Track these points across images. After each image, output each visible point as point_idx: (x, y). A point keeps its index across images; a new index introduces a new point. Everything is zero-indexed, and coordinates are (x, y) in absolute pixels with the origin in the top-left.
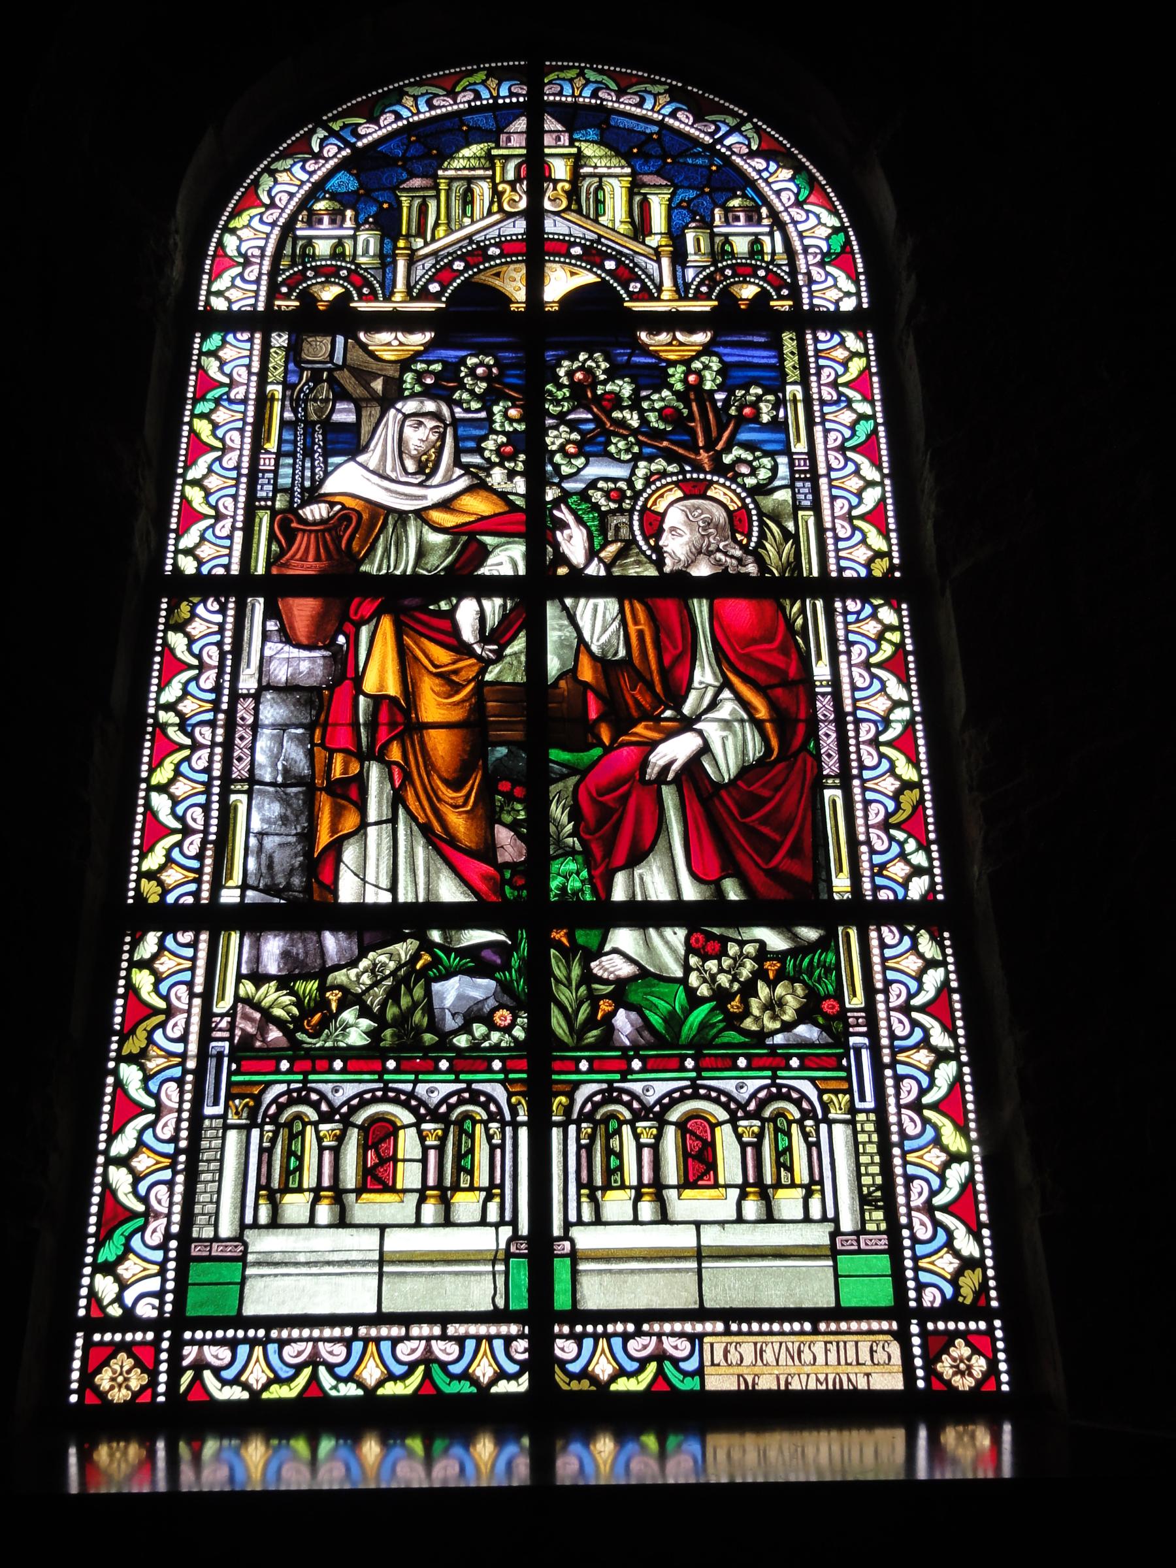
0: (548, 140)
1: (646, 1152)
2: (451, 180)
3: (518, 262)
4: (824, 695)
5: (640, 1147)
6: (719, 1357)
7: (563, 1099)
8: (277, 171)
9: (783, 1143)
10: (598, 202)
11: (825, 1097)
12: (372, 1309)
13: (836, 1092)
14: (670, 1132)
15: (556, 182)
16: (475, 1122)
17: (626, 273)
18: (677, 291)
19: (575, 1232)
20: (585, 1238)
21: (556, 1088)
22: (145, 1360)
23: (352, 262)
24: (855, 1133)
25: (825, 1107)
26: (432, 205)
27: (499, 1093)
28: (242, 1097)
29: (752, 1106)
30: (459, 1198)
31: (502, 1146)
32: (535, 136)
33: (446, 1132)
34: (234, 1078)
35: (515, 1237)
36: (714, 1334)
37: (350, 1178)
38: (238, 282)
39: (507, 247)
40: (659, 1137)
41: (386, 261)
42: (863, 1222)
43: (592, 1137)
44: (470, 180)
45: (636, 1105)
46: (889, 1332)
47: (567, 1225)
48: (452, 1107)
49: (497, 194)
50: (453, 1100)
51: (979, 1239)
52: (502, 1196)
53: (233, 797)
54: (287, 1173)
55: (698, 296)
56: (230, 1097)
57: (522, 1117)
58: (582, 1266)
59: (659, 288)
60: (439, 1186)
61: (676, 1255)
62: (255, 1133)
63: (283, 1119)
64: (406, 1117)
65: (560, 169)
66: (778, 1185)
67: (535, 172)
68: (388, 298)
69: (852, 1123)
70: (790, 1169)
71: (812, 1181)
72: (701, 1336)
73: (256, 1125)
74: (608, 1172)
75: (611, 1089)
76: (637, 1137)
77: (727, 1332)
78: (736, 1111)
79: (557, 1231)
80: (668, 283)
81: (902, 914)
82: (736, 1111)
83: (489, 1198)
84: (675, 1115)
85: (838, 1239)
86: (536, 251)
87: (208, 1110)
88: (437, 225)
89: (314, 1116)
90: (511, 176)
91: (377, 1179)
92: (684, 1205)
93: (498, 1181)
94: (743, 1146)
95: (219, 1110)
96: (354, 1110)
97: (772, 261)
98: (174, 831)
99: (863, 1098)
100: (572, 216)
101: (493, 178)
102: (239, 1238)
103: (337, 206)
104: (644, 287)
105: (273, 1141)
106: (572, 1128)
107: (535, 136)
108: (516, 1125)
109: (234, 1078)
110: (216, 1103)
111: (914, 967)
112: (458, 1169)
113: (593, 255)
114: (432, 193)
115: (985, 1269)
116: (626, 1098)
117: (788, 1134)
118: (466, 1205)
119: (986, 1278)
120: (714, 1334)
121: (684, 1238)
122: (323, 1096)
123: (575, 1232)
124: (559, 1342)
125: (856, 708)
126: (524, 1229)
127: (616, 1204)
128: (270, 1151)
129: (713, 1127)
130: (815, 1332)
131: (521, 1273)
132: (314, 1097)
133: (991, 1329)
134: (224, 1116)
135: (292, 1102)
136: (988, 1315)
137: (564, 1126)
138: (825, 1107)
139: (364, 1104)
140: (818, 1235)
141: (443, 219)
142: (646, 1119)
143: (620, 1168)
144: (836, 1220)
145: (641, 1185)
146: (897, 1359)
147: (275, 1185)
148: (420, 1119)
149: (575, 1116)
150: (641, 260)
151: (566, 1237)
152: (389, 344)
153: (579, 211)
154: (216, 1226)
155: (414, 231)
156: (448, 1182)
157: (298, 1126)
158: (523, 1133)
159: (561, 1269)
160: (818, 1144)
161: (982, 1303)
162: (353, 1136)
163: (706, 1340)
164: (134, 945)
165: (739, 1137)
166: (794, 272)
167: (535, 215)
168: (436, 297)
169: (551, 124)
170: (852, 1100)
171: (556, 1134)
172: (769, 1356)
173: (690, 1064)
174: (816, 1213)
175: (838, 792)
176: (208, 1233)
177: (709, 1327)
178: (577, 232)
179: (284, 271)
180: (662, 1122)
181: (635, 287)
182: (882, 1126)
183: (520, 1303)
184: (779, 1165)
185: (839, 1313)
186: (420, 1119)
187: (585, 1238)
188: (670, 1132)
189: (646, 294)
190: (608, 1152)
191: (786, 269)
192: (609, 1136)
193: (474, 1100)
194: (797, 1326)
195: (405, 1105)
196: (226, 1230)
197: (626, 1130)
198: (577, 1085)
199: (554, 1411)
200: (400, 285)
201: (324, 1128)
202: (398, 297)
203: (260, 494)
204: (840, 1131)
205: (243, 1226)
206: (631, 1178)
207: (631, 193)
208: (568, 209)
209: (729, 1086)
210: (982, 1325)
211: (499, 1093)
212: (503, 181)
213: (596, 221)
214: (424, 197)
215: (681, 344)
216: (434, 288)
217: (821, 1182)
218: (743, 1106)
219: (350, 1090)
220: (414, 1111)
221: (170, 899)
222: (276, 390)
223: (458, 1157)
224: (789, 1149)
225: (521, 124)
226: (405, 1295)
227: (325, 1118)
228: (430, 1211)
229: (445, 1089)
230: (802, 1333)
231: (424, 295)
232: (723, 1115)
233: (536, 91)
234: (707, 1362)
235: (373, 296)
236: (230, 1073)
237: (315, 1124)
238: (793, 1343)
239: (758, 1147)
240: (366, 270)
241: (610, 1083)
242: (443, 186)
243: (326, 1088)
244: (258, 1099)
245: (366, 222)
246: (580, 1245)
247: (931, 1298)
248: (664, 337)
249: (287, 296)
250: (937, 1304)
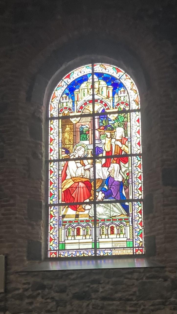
0: (95, 80)
1: (107, 230)
2: (82, 89)
3: (91, 104)
5: (106, 230)
6: (114, 252)
7: (98, 225)
8: (57, 90)
9: (122, 229)
10: (102, 92)
11: (127, 223)
12: (78, 248)
13: (128, 223)
14: (109, 228)
15: (96, 88)
16: (88, 228)
17: (106, 105)
18: (113, 108)
19: (99, 239)
20: (100, 240)
21: (97, 223)
22: (55, 253)
23: (69, 106)
24: (130, 228)
25: (126, 225)
26: (79, 94)
27: (91, 224)
28: (64, 226)
29: (119, 225)
30: (87, 236)
31: (91, 230)
32: (93, 79)
33: (85, 229)
34: (63, 224)
35: (93, 240)
37: (75, 234)
38: (54, 111)
39: (90, 102)
40: (108, 229)
41: (73, 106)
42: (130, 238)
43: (101, 229)
44: (84, 89)
45: (106, 225)
47: (98, 239)
48: (86, 226)
49: (88, 91)
50: (86, 225)
51: (142, 239)
52: (91, 236)
53: (59, 189)
54: (69, 234)
55: (116, 108)
56: (62, 226)
57: (93, 227)
58: (100, 243)
59: (110, 107)
60: (85, 235)
61: (110, 242)
62: (65, 230)
63: (68, 228)
64: (81, 227)
65: (96, 85)
66: (121, 234)
67: (93, 87)
68: (74, 113)
69: (129, 226)
70: (122, 232)
71: (125, 233)
73: (65, 229)
74: (103, 233)
75: (103, 223)
76: (106, 229)
77: (115, 250)
78: (117, 225)
79: (97, 239)
80: (112, 106)
82: (117, 225)
83: (90, 236)
84: (110, 226)
86: (93, 101)
87: (60, 227)
88: (80, 98)
89: (71, 228)
90: (90, 88)
91: (78, 234)
92: (111, 236)
93: (91, 234)
94: (117, 230)
95: (61, 227)
96: (75, 227)
97: (127, 101)
98: (54, 194)
100: (99, 95)
101: (87, 88)
102: (64, 241)
103: (66, 96)
104: (108, 108)
105: (67, 231)
106: (99, 228)
107: (93, 79)
108: (93, 228)
109: (63, 224)
110: (61, 226)
111: (138, 207)
112: (87, 233)
113: (101, 102)
114: (79, 92)
115: (142, 242)
116: (105, 224)
117: (122, 228)
118: (88, 237)
119: (143, 244)
121: (110, 240)
122: (72, 225)
123: (99, 239)
124: (97, 252)
125: (134, 173)
126: (94, 239)
127: (103, 236)
128: (67, 232)
129: (114, 227)
130: (124, 250)
131: (93, 244)
132: (71, 225)
133: (143, 249)
134: (62, 228)
135: (69, 226)
136: (142, 247)
137: (98, 228)
138: (126, 225)
139: (76, 226)
140: (125, 239)
141: (81, 97)
142: (107, 227)
143: (104, 232)
144: (127, 238)
145: (106, 234)
147: (68, 235)
148: (83, 227)
149: (99, 227)
150: (108, 102)
151: (98, 240)
152: (74, 120)
153: (100, 94)
154: (62, 240)
155: (77, 100)
156: (86, 234)
157: (69, 229)
158: (94, 228)
159: (98, 244)
160: (125, 229)
161: (142, 246)
162: (76, 229)
164: (51, 208)
165: (117, 228)
166: (130, 103)
167: (93, 95)
168: (80, 112)
169: (95, 77)
170: (129, 224)
171: (97, 228)
172: (119, 252)
173: (112, 220)
174: (125, 237)
176: (61, 241)
178: (99, 98)
179: (60, 108)
180: (108, 226)
181: (107, 107)
182: (133, 227)
183: (93, 247)
184: (121, 231)
186: (83, 227)
187: (100, 240)
188: (109, 228)
189: (108, 109)
190: (103, 230)
191: (129, 102)
192: (103, 228)
193: (88, 225)
195: (81, 226)
196: (63, 240)
197: (105, 228)
198: (99, 223)
199: (96, 258)
200: (76, 110)
201: (72, 229)
202: (75, 112)
203: (60, 147)
204: (128, 228)
205: (65, 240)
206: (105, 233)
207: (107, 89)
208: (98, 93)
209: (116, 223)
210: (142, 249)
211: (91, 224)
212: (89, 89)
213: (102, 95)
214: (78, 93)
216: (80, 110)
217: (125, 233)
218: (117, 225)
219: (75, 225)
220: (82, 226)
221: (54, 203)
222: (60, 130)
223: (87, 232)
224: (122, 230)
225: (91, 77)
226: (82, 247)
227: (72, 228)
228: (84, 238)
229: (85, 224)
231: (79, 112)
232: (115, 226)
233: (93, 69)
234: (113, 253)
235: (72, 112)
236: (62, 223)
237: (71, 228)
238: (122, 251)
239: (119, 229)
240: (71, 107)
241: (103, 222)
242: (80, 91)
243: (73, 224)
244: (65, 226)
245: (70, 99)
246: (100, 241)
247: (137, 246)
249: (61, 114)
250: (137, 246)
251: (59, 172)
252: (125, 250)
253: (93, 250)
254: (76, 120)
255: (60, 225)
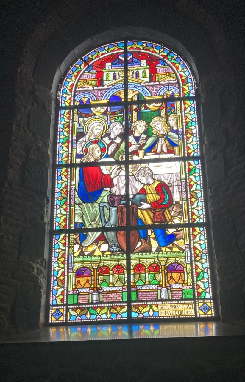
4: (183, 182)
36: (160, 304)
46: (192, 303)
72: (158, 304)
81: (199, 225)
85: (183, 287)
95: (72, 267)
99: (188, 261)
110: (71, 266)
120: (160, 304)
130: (178, 303)
131: (125, 294)
146: (194, 308)
163: (159, 305)
175: (186, 202)
177: (159, 303)
185: (182, 299)
194: (175, 302)
203: (73, 146)
215: (155, 106)
230: (176, 303)
248: (152, 105)
251: (72, 182)
252: (181, 303)
253: (125, 304)
254: (100, 111)
255: (70, 265)
